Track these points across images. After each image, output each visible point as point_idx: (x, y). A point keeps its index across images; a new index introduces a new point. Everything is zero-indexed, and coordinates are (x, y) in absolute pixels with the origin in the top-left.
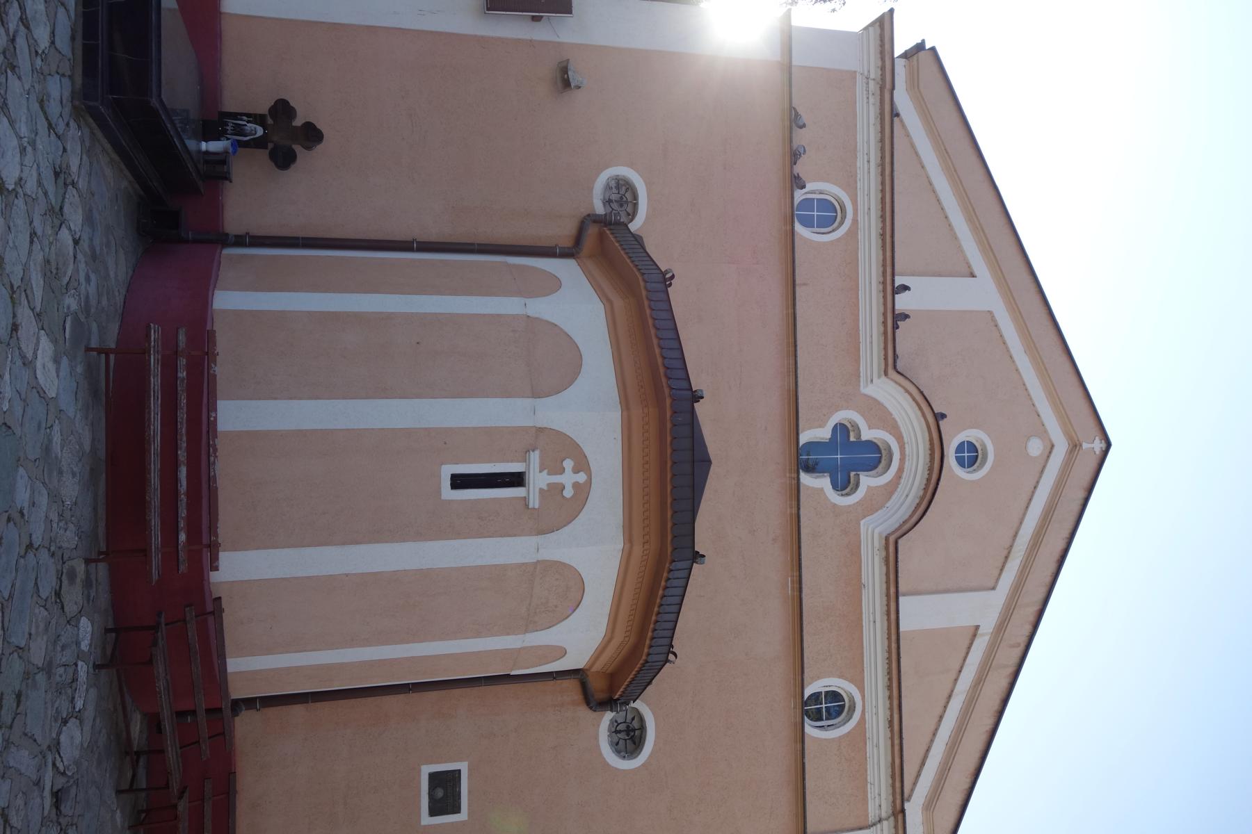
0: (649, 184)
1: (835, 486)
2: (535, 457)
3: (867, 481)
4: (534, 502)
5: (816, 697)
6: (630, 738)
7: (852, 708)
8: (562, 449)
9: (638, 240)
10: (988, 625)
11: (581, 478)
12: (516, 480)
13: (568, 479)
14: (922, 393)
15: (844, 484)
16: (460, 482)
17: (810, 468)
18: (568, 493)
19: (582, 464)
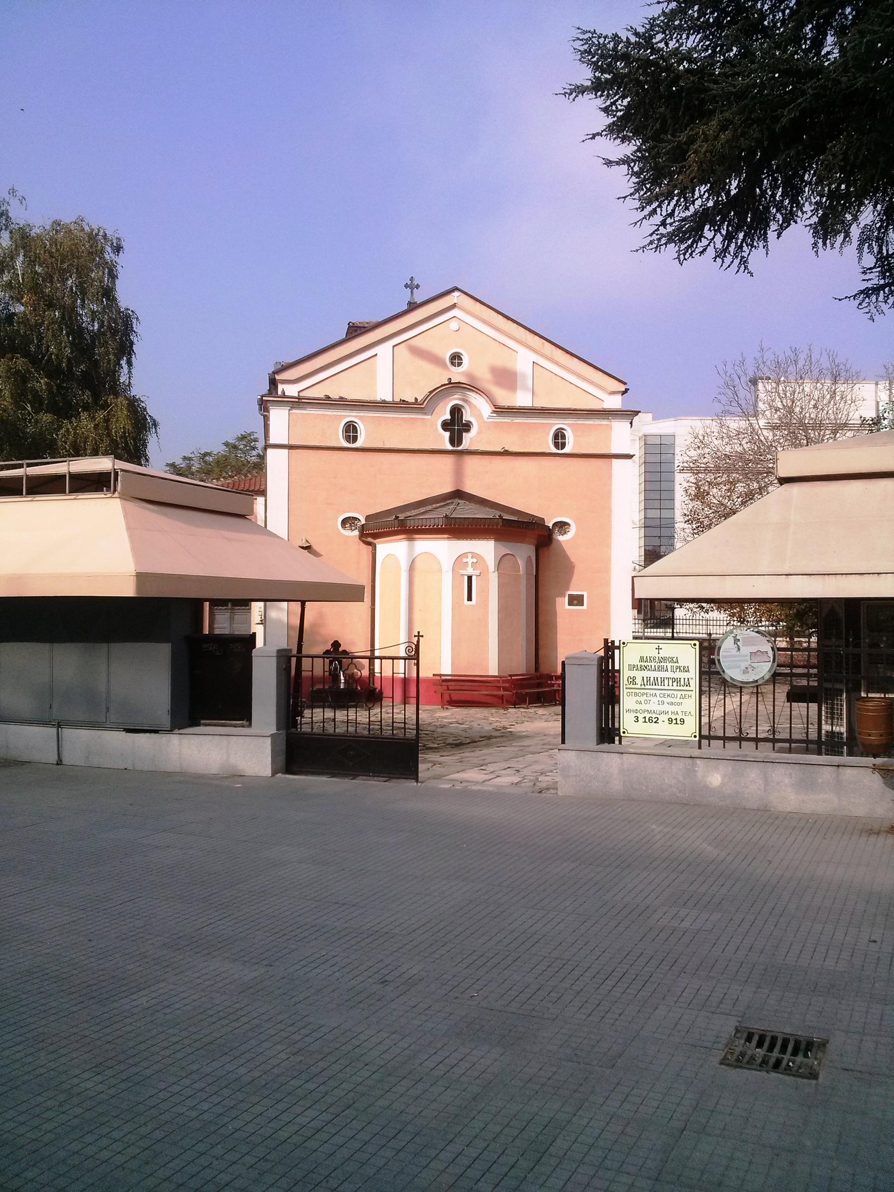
0: (344, 512)
1: (468, 431)
2: (462, 572)
3: (467, 416)
4: (477, 572)
5: (556, 445)
6: (562, 526)
7: (563, 429)
8: (459, 562)
9: (368, 518)
10: (535, 357)
11: (470, 555)
12: (470, 578)
13: (470, 560)
14: (431, 392)
15: (467, 427)
16: (470, 598)
17: (460, 442)
18: (475, 560)
19: (465, 555)
